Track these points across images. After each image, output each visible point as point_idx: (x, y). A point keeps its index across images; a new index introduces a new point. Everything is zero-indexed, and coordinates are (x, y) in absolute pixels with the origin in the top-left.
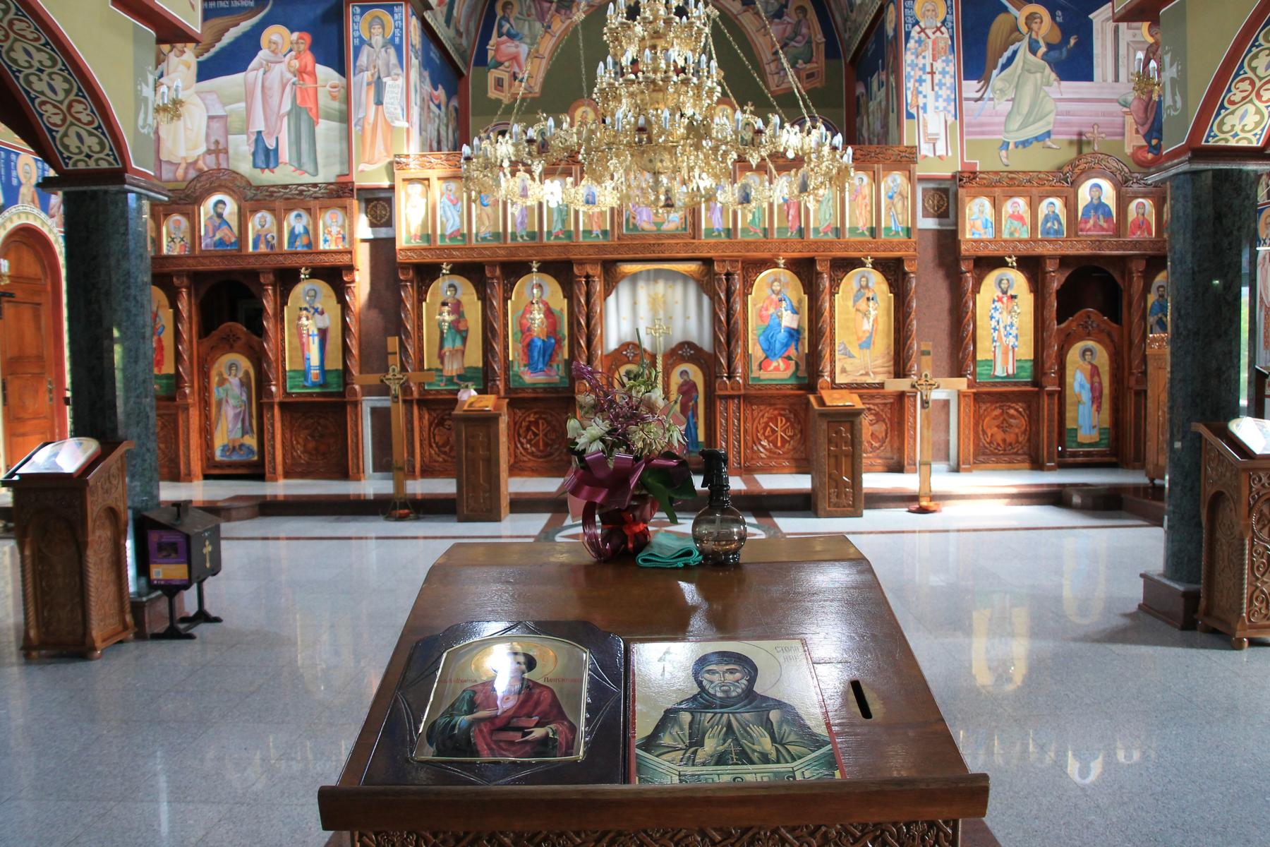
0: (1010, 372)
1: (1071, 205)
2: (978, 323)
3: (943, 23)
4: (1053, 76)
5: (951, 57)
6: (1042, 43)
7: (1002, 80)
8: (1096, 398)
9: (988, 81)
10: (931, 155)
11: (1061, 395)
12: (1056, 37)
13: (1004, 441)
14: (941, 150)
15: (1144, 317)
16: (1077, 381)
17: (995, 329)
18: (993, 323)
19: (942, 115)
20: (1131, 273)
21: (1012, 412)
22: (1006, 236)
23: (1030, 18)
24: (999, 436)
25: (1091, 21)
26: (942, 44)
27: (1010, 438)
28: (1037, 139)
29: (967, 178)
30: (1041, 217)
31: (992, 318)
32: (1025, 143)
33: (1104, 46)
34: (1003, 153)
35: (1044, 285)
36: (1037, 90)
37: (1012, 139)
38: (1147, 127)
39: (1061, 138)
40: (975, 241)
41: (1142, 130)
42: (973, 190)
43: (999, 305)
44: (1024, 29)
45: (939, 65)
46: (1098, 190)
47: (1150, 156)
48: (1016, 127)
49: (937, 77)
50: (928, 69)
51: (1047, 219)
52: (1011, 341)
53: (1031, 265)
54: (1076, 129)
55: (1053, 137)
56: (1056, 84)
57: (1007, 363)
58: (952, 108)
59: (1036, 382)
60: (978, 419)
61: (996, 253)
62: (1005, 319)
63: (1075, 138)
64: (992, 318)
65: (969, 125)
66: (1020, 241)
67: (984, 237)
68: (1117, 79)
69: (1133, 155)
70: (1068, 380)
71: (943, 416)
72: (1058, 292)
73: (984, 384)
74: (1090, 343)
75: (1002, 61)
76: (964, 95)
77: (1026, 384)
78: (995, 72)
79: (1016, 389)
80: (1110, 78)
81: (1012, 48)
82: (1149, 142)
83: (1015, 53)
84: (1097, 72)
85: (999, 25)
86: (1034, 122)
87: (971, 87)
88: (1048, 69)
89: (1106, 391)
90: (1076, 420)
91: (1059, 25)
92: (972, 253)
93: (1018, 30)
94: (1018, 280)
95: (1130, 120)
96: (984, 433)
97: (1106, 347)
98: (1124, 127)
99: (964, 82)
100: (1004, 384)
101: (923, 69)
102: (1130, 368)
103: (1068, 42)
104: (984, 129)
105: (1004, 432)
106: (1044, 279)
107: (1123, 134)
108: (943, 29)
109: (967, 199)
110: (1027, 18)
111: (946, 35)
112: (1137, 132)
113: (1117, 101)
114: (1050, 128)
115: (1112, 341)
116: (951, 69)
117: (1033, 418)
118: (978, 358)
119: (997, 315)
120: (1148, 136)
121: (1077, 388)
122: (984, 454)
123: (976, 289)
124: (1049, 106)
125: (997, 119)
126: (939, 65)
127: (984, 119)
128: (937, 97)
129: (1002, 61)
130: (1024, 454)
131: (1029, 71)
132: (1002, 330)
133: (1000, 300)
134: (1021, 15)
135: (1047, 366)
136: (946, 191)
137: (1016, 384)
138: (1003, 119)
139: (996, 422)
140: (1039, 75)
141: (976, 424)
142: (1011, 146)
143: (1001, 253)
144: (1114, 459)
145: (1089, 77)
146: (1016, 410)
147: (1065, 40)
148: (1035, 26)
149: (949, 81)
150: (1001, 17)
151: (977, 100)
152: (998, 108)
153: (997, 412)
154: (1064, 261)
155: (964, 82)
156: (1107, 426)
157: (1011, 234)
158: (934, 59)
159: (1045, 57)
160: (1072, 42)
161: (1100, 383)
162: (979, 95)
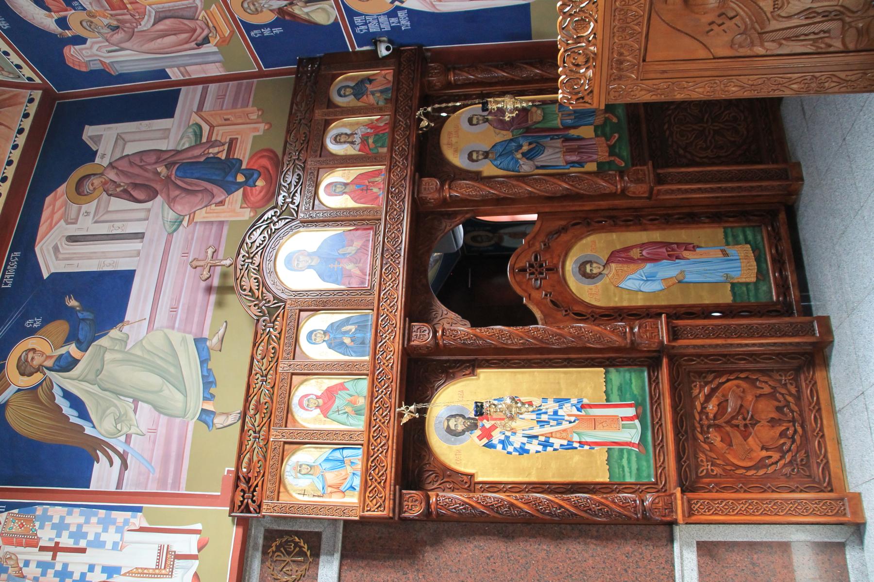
0: (631, 412)
1: (322, 303)
2: (533, 479)
4: (114, 333)
5: (39, 510)
6: (63, 351)
7: (101, 419)
8: (672, 252)
9: (100, 444)
10: (197, 562)
11: (676, 314)
12: (60, 327)
13: (773, 422)
14: (186, 544)
15: (523, 178)
16: (642, 284)
17: (546, 444)
18: (534, 447)
19: (129, 536)
20: (444, 202)
21: (712, 407)
22: (359, 424)
23: (24, 369)
24: (765, 433)
25: (53, 276)
27: (766, 410)
28: (204, 362)
29: (247, 492)
30: (334, 356)
31: (523, 451)
32: (208, 382)
34: (219, 421)
35: (462, 350)
36: (130, 360)
37: (196, 403)
38: (216, 190)
39: (211, 322)
40: (365, 485)
41: (220, 194)
42: (268, 485)
43: (497, 436)
45: (46, 536)
46: (303, 260)
47: (260, 183)
48: (179, 396)
49: (66, 541)
50: (47, 556)
51: (337, 345)
52: (568, 410)
53: (420, 375)
54: (200, 295)
55: (206, 334)
56: (126, 329)
57: (614, 418)
58: (120, 516)
59: (650, 361)
60: (737, 480)
61: (392, 444)
62: (525, 423)
63: (213, 298)
64: (523, 451)
65: (163, 482)
66: (372, 396)
67: (359, 465)
68: (139, 236)
69: (254, 208)
70: (639, 301)
71: (733, 556)
72: (474, 325)
73: (660, 468)
74: (570, 266)
75: (74, 419)
76: (113, 489)
77: (654, 381)
78: (89, 430)
79: (667, 402)
80: (136, 245)
82: (240, 185)
83: (67, 395)
84: (123, 265)
85: (24, 422)
86: (179, 367)
87: (104, 475)
88: (103, 342)
89: (656, 236)
90: (714, 286)
91: (45, 322)
92: (387, 493)
93: (34, 389)
94: (451, 398)
95: (201, 215)
96: (761, 464)
97: (578, 238)
98: (212, 223)
99: (93, 487)
100: (657, 426)
101: (44, 566)
102: (612, 195)
103: (73, 308)
104: (173, 454)
105: (755, 422)
106: (447, 350)
107: (222, 223)
109: (283, 498)
110: (22, 374)
112: (222, 203)
113: (171, 234)
114: (190, 338)
115: (564, 229)
116: (57, 513)
117: (722, 365)
118: (604, 478)
119: (517, 440)
120: (229, 188)
121: (655, 286)
122: (807, 465)
123: (467, 482)
124: (157, 339)
125: (162, 430)
126: (46, 536)
127: (158, 452)
128: (98, 544)
129: (74, 419)
130: (796, 380)
131: (99, 372)
132: (547, 429)
133: (487, 434)
134: (18, 381)
135: (616, 340)
136: (270, 535)
137: (656, 401)
138: (163, 419)
139: (737, 438)
140: (108, 356)
141: (746, 484)
142: (209, 406)
143: (391, 432)
144: (782, 216)
145: (128, 277)
146: (707, 402)
147: (67, 314)
149: (75, 518)
151: (125, 465)
152: (143, 428)
153: (715, 437)
154: (416, 311)
155: (93, 487)
156: (719, 232)
157: (357, 412)
158: (32, 543)
159: (83, 347)
160: (73, 303)
161: (642, 246)
162: (117, 461)
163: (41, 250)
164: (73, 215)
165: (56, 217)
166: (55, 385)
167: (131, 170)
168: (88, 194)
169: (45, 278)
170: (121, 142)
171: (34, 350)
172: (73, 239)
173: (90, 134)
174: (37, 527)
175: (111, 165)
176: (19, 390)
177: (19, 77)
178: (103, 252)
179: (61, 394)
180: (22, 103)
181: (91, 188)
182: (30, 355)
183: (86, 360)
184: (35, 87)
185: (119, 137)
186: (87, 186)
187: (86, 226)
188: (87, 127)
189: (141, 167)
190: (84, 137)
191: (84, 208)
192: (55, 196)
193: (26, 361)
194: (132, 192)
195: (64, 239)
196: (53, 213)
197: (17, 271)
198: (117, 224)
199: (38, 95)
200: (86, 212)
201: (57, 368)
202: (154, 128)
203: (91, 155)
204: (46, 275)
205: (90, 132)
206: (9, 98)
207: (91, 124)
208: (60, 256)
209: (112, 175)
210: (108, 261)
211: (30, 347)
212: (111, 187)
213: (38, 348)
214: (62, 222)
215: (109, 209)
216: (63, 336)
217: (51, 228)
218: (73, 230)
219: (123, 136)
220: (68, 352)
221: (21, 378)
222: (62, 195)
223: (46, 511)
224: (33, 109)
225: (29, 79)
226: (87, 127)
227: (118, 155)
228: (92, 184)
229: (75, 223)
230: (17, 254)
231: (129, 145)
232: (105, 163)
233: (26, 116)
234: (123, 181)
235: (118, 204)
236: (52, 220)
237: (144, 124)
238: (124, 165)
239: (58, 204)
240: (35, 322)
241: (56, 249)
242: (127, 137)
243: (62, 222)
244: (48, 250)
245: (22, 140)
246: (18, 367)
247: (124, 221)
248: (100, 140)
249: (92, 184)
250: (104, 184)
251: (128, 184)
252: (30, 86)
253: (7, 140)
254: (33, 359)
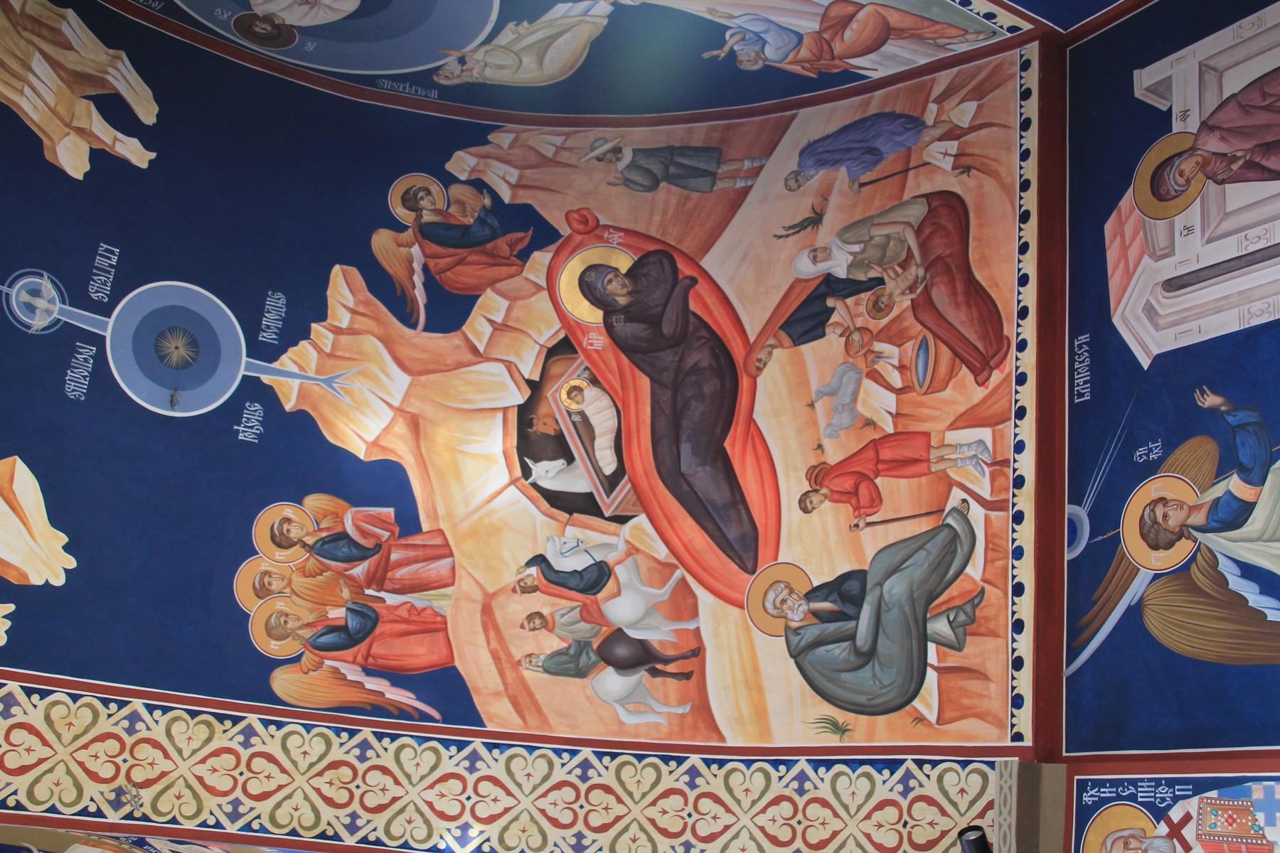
3: (1159, 813)
6: (1218, 491)
12: (1201, 450)
23: (1156, 538)
26: (1219, 823)
33: (1217, 307)
44: (1183, 549)
81: (1237, 583)
83: (1249, 571)
85: (1180, 630)
91: (1170, 447)
93: (1185, 569)
103: (1213, 410)
108: (1176, 814)
110: (1155, 547)
111: (1192, 805)
134: (1147, 561)
147: (1207, 423)
148: (1175, 518)
150: (1155, 624)
159: (1256, 477)
160: (1211, 400)
163: (1124, 319)
164: (1162, 241)
165: (1133, 253)
166: (1220, 557)
167: (1250, 121)
168: (1179, 194)
169: (1146, 368)
170: (1211, 77)
171: (1163, 500)
172: (1174, 285)
173: (1146, 84)
174: (1261, 822)
175: (1206, 126)
176: (1156, 577)
177: (994, 33)
178: (1240, 293)
179: (1238, 572)
180: (1012, 76)
181: (1181, 181)
182: (1159, 511)
183: (1266, 500)
184: (1026, 39)
185: (1204, 68)
186: (1173, 181)
187: (1194, 252)
188: (1136, 72)
189: (1266, 108)
190: (1138, 94)
191: (1179, 222)
192: (1119, 215)
193: (1155, 522)
194: (1264, 163)
195: (1159, 289)
196: (1125, 248)
197: (1091, 368)
198: (1252, 233)
199: (1032, 51)
200: (1185, 228)
201: (1214, 524)
202: (1269, 25)
203: (1162, 121)
204: (1145, 363)
205: (1144, 79)
206: (990, 75)
207: (1142, 65)
208: (1162, 322)
209: (1213, 144)
210: (1256, 306)
211: (1155, 496)
212: (1218, 166)
213: (1169, 495)
214: (1146, 260)
215: (1228, 210)
216: (1209, 466)
217: (1129, 275)
218: (1170, 268)
219: (1212, 63)
220: (1229, 493)
221: (1154, 554)
222: (1131, 211)
223: (1269, 793)
224: (1032, 79)
225: (1012, 29)
226: (1136, 72)
227: (1212, 102)
228: (1181, 174)
229: (1171, 253)
230: (1084, 338)
231: (1228, 76)
232: (1193, 125)
233: (1026, 95)
234: (1240, 147)
235: (1241, 194)
236: (1127, 265)
237: (1247, 25)
238: (1232, 117)
239: (1128, 229)
240: (1150, 450)
241: (1150, 311)
242: (1221, 62)
243: (1146, 260)
244: (1137, 318)
245: (1032, 140)
246: (1144, 536)
247: (1265, 221)
248: (1169, 88)
249: (1181, 174)
250: (1203, 166)
251: (1252, 150)
252: (1018, 39)
253: (1009, 149)
254: (1165, 516)
